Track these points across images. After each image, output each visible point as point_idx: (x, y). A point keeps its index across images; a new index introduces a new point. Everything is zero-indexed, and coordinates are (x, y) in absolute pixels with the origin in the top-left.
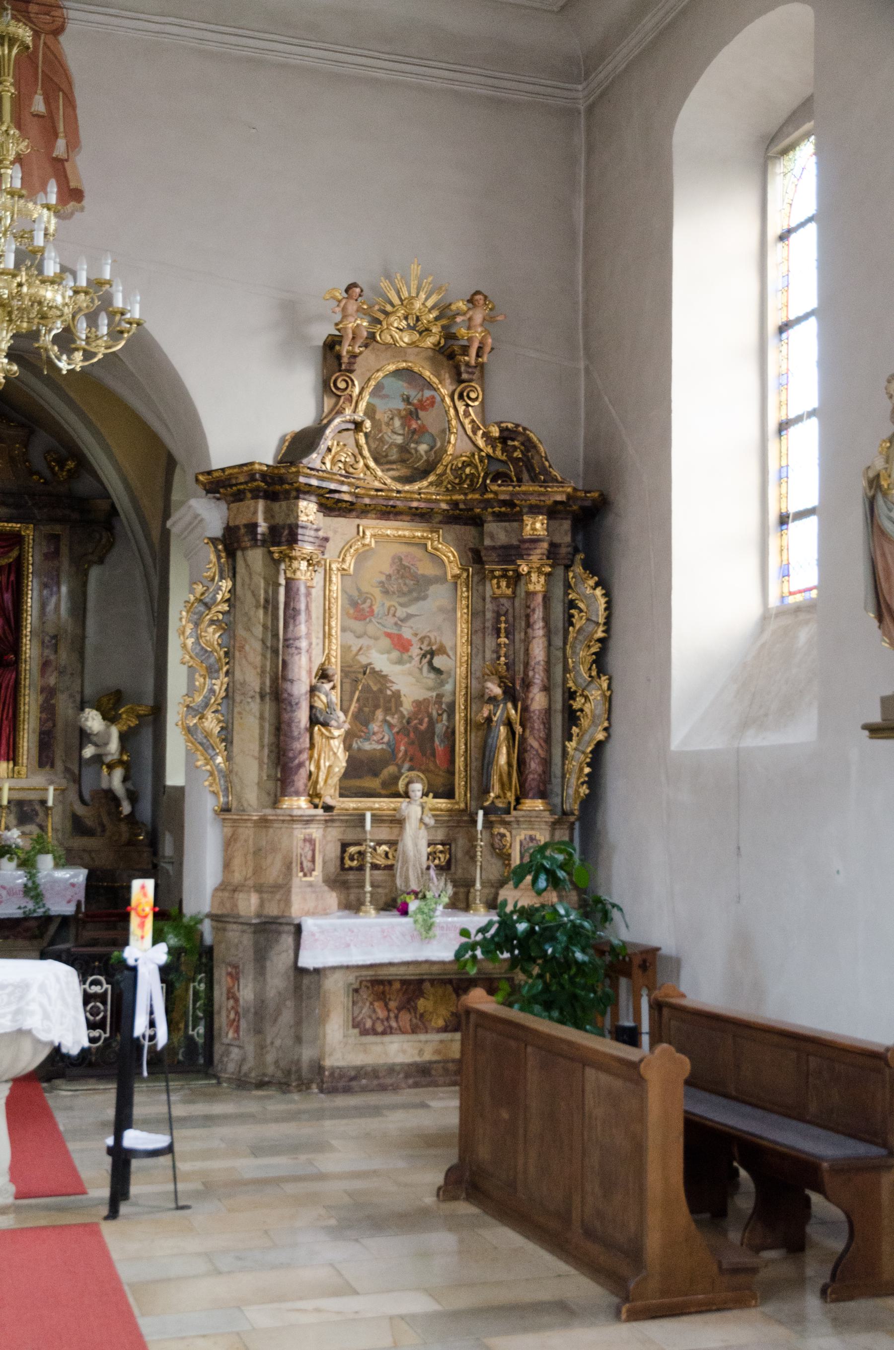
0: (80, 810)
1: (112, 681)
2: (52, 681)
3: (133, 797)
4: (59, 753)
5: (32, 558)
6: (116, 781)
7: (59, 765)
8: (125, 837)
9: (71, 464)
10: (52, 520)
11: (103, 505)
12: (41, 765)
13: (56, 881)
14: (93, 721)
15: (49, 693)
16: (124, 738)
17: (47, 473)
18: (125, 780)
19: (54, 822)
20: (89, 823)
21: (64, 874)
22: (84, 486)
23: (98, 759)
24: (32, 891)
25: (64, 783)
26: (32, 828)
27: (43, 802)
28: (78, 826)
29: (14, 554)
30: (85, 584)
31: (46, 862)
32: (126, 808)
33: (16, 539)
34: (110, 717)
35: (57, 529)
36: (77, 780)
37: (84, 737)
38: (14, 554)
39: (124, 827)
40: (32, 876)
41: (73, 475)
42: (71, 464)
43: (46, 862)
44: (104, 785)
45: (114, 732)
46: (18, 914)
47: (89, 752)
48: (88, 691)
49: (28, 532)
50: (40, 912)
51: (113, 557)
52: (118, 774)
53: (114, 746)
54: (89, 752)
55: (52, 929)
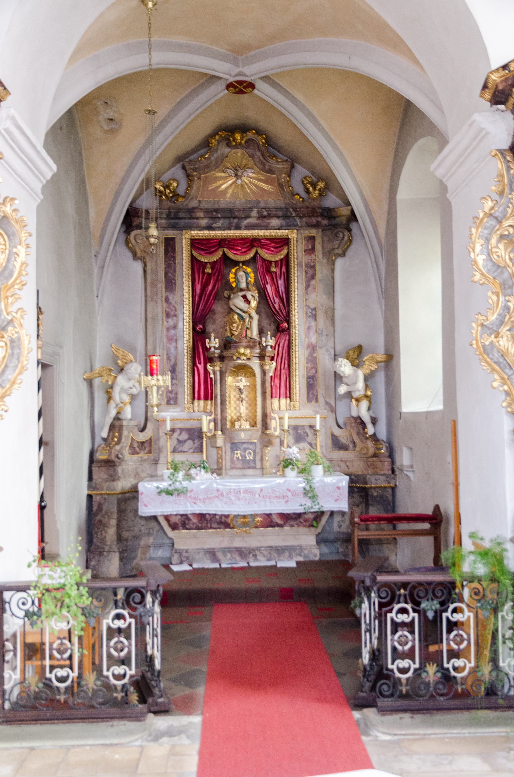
0: (337, 432)
1: (355, 341)
2: (313, 339)
3: (374, 421)
4: (321, 391)
5: (297, 252)
6: (363, 411)
7: (321, 399)
8: (371, 451)
9: (321, 185)
10: (310, 226)
11: (345, 211)
12: (309, 400)
13: (325, 485)
14: (345, 367)
15: (312, 348)
16: (367, 379)
17: (304, 195)
18: (369, 409)
19: (322, 441)
20: (344, 441)
21: (329, 480)
22: (331, 201)
23: (349, 395)
24: (309, 493)
25: (326, 413)
26: (304, 445)
27: (312, 427)
28: (337, 444)
29: (285, 252)
30: (333, 270)
31: (318, 471)
32: (370, 430)
33: (285, 242)
34: (356, 363)
35: (313, 232)
36: (333, 410)
37: (338, 377)
38: (285, 252)
39: (370, 444)
40: (308, 481)
41: (322, 194)
42: (321, 185)
43: (318, 471)
44: (354, 414)
45: (361, 374)
46: (300, 510)
47: (342, 389)
48: (338, 348)
49: (293, 235)
50: (316, 508)
51: (350, 253)
52: (364, 404)
53: (361, 385)
54: (342, 389)
55: (324, 519)
